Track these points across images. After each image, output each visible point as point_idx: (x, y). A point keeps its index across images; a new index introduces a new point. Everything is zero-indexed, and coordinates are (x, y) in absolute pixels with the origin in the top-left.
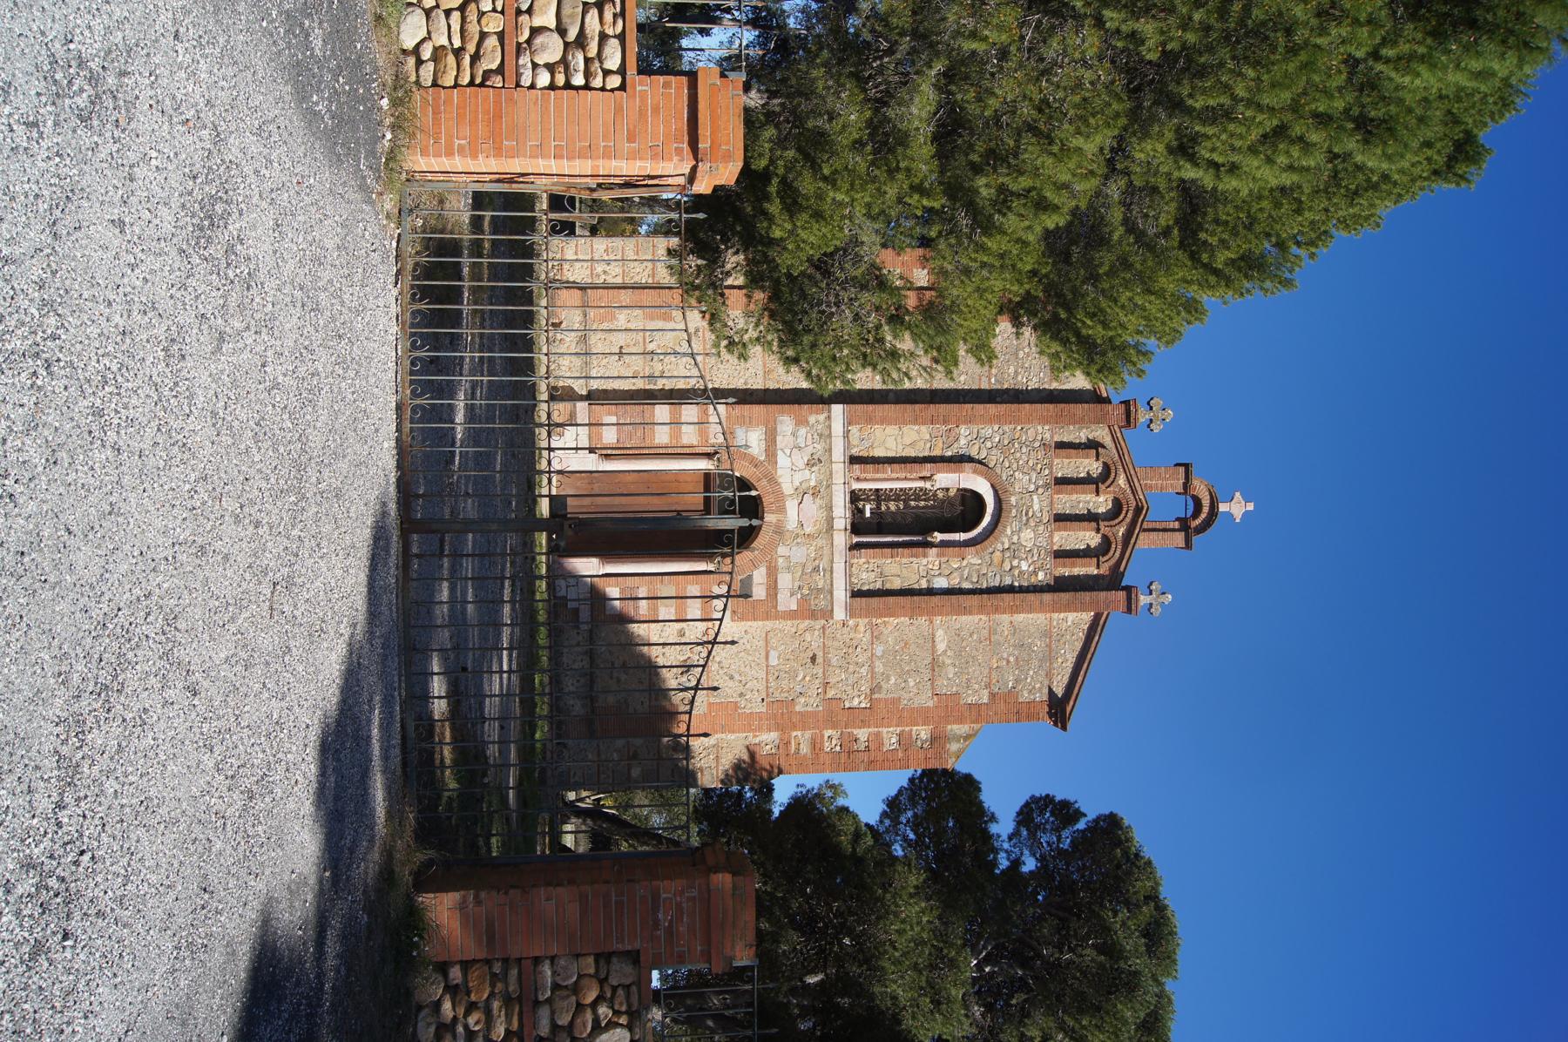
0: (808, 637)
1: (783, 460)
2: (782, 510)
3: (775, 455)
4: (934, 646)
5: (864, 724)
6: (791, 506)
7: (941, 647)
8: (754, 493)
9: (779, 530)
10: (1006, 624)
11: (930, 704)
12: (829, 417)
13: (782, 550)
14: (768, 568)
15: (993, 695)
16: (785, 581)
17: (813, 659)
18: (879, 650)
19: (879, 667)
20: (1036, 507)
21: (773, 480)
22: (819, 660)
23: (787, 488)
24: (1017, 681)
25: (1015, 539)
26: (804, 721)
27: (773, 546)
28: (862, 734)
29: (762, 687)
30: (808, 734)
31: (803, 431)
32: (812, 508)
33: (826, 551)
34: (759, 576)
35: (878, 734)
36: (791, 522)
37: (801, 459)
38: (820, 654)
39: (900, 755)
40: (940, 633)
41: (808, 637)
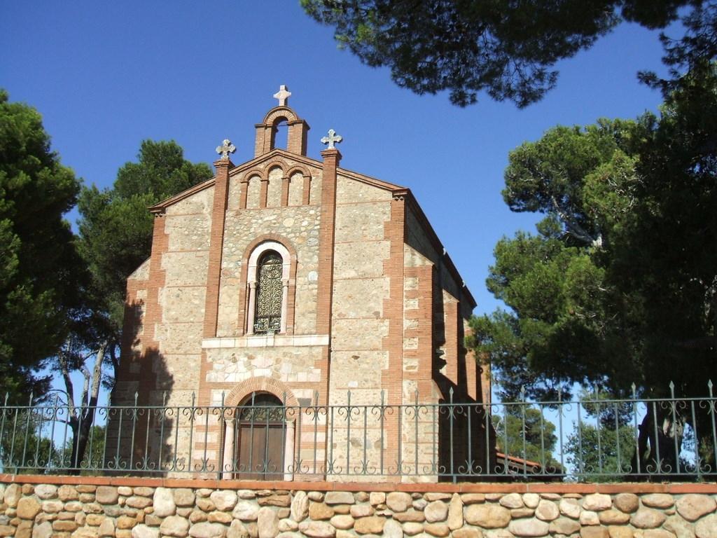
0: (341, 361)
1: (231, 379)
2: (260, 379)
3: (228, 383)
4: (353, 279)
5: (400, 323)
6: (258, 373)
7: (353, 274)
8: (254, 395)
9: (272, 381)
10: (340, 232)
11: (388, 279)
12: (209, 349)
13: (283, 379)
14: (294, 387)
15: (386, 238)
16: (302, 377)
17: (356, 357)
18: (352, 314)
19: (364, 314)
20: (272, 218)
21: (242, 385)
22: (356, 354)
23: (248, 376)
24: (378, 223)
25: (288, 230)
26: (396, 363)
27: (281, 385)
28: (407, 324)
29: (371, 391)
30: (405, 360)
31: (216, 366)
32: (259, 359)
33: (286, 350)
34: (298, 394)
35: (409, 313)
36: (268, 373)
37: (232, 367)
38: (353, 353)
39: (422, 298)
40: (344, 275)
41: (341, 361)
